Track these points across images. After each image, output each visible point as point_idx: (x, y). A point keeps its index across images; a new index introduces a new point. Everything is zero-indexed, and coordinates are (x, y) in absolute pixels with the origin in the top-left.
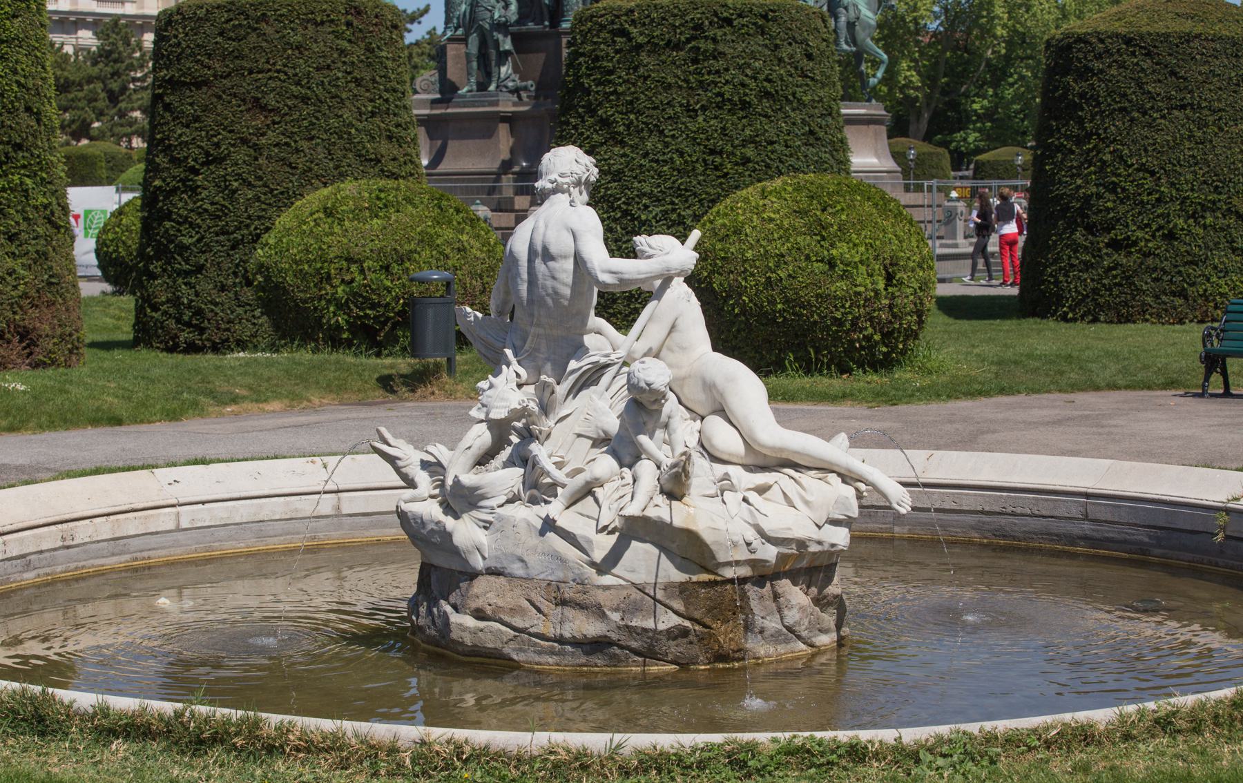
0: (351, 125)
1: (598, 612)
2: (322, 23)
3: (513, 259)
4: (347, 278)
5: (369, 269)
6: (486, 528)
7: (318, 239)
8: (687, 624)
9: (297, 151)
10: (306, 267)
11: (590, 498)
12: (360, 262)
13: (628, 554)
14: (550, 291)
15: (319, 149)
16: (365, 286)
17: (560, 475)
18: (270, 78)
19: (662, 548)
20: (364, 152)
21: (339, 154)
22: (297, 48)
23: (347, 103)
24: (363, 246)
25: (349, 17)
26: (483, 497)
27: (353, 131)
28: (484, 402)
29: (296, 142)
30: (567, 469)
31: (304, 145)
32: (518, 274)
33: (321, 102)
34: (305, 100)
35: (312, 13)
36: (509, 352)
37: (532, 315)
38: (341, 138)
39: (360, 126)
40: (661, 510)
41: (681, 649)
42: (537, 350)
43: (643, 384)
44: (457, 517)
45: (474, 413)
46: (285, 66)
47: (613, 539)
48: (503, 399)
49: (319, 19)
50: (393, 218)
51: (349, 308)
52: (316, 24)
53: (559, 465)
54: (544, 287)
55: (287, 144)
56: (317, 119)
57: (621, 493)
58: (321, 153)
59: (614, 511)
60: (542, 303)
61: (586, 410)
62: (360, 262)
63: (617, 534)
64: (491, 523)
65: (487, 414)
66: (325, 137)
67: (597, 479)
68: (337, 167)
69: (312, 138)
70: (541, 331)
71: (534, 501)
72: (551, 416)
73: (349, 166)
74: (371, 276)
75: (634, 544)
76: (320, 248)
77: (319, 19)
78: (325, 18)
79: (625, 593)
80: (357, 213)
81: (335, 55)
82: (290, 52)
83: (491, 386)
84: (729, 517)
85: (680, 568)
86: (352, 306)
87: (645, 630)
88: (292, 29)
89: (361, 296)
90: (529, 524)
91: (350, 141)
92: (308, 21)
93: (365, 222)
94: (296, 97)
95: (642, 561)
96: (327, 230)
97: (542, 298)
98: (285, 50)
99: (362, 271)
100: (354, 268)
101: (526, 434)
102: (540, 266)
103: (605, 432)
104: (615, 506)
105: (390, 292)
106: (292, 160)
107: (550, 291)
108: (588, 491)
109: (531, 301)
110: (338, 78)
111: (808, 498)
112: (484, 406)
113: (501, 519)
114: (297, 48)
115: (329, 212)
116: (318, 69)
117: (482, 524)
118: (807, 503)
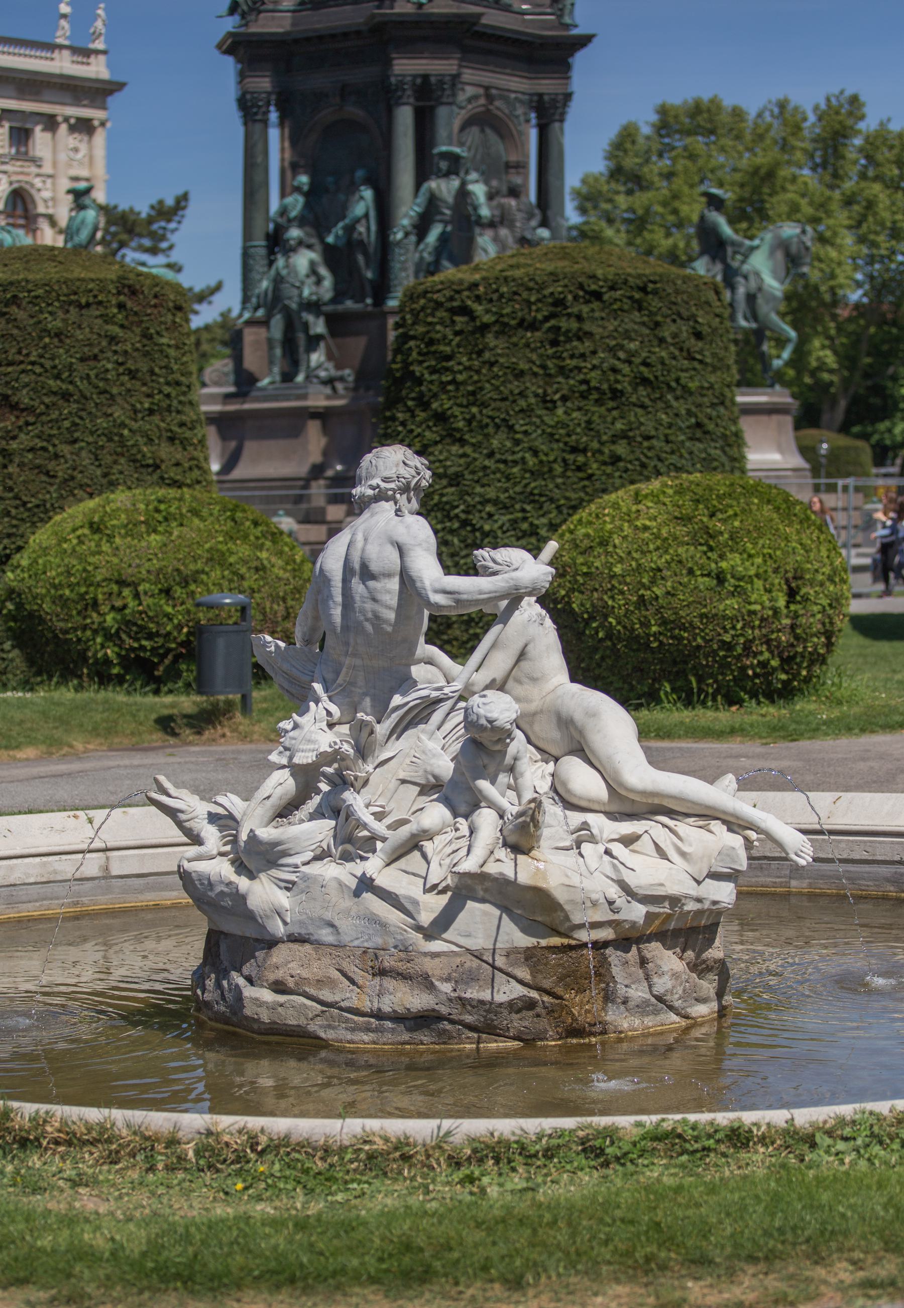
0: (123, 425)
1: (426, 983)
2: (88, 305)
3: (324, 579)
4: (119, 603)
5: (146, 593)
7: (82, 559)
8: (534, 994)
9: (56, 456)
10: (67, 592)
11: (416, 854)
12: (135, 585)
13: (462, 917)
14: (370, 615)
15: (84, 454)
16: (141, 613)
17: (379, 827)
18: (23, 371)
19: (505, 909)
20: (139, 457)
21: (109, 459)
22: (57, 335)
23: (119, 400)
24: (138, 566)
25: (122, 298)
27: (126, 432)
29: (54, 446)
30: (388, 820)
31: (65, 449)
32: (330, 596)
33: (86, 398)
34: (66, 396)
35: (75, 293)
37: (347, 644)
38: (110, 440)
39: (135, 425)
40: (504, 865)
41: (526, 1023)
42: (352, 684)
46: (41, 356)
47: (444, 899)
49: (83, 301)
50: (176, 533)
51: (120, 638)
52: (81, 307)
53: (379, 816)
54: (363, 611)
55: (44, 449)
56: (81, 418)
57: (454, 847)
58: (86, 459)
59: (445, 868)
60: (359, 629)
61: (413, 752)
62: (135, 585)
63: (449, 894)
66: (91, 439)
67: (425, 831)
68: (105, 475)
69: (75, 441)
70: (358, 662)
72: (370, 759)
73: (121, 473)
74: (147, 601)
75: (470, 904)
76: (85, 570)
77: (83, 301)
78: (91, 300)
79: (458, 960)
80: (130, 529)
81: (104, 343)
82: (47, 340)
84: (580, 870)
85: (525, 931)
86: (124, 636)
87: (482, 1002)
88: (51, 313)
89: (135, 624)
91: (122, 442)
92: (71, 303)
93: (141, 537)
94: (55, 393)
95: (481, 926)
96: (93, 548)
97: (360, 624)
98: (41, 338)
99: (137, 596)
100: (126, 592)
102: (358, 587)
103: (435, 777)
104: (447, 861)
105: (170, 619)
106: (50, 467)
107: (370, 615)
108: (414, 844)
109: (346, 627)
110: (107, 370)
114: (57, 335)
115: (95, 528)
116: (82, 360)
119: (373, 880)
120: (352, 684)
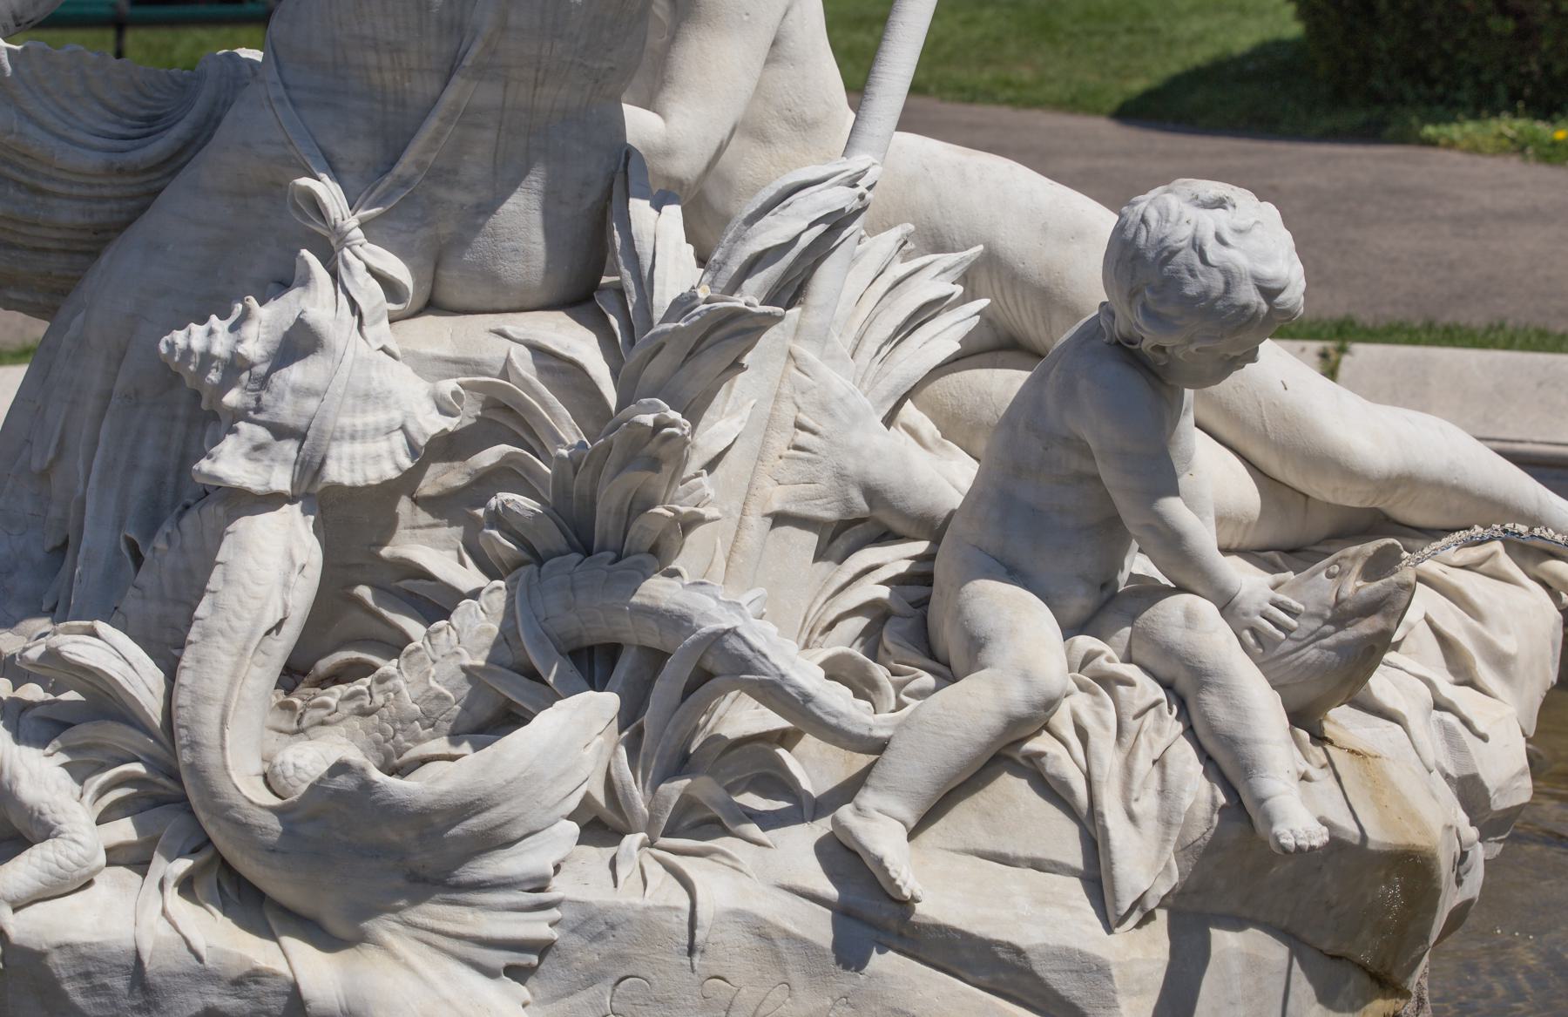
6: (517, 973)
26: (495, 841)
28: (286, 412)
36: (327, 191)
42: (442, 175)
43: (1248, 295)
44: (327, 941)
45: (230, 463)
48: (369, 398)
59: (1151, 826)
61: (788, 413)
63: (1162, 916)
64: (543, 948)
65: (310, 469)
71: (700, 823)
83: (300, 342)
90: (763, 932)
101: (549, 537)
103: (872, 493)
108: (1007, 753)
111: (1508, 644)
112: (280, 432)
113: (594, 924)
117: (500, 958)
118: (1501, 662)
119: (906, 905)
120: (442, 175)
